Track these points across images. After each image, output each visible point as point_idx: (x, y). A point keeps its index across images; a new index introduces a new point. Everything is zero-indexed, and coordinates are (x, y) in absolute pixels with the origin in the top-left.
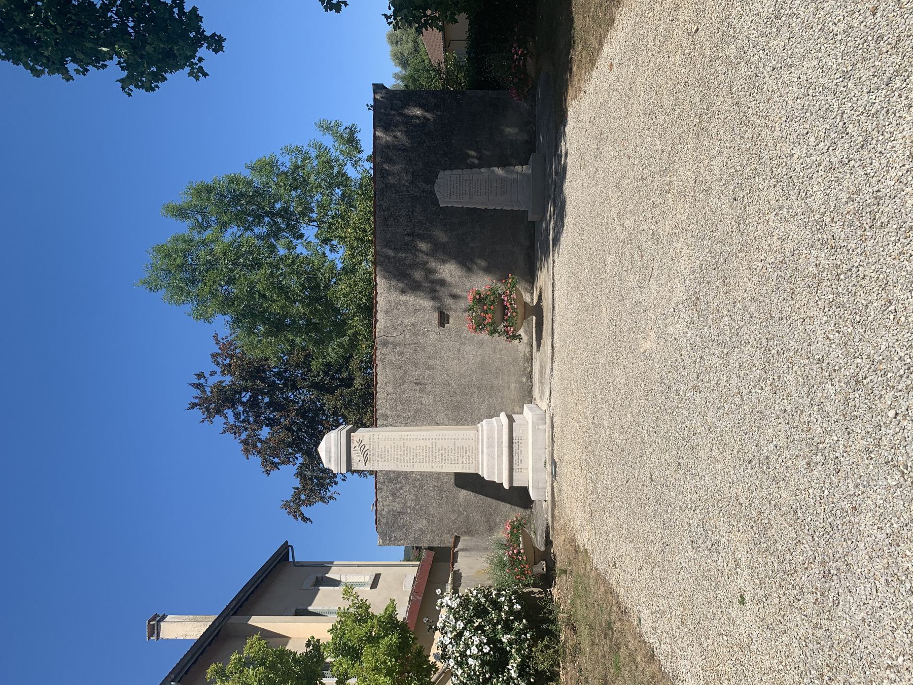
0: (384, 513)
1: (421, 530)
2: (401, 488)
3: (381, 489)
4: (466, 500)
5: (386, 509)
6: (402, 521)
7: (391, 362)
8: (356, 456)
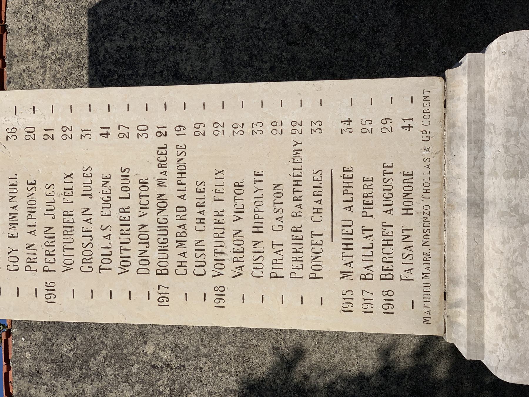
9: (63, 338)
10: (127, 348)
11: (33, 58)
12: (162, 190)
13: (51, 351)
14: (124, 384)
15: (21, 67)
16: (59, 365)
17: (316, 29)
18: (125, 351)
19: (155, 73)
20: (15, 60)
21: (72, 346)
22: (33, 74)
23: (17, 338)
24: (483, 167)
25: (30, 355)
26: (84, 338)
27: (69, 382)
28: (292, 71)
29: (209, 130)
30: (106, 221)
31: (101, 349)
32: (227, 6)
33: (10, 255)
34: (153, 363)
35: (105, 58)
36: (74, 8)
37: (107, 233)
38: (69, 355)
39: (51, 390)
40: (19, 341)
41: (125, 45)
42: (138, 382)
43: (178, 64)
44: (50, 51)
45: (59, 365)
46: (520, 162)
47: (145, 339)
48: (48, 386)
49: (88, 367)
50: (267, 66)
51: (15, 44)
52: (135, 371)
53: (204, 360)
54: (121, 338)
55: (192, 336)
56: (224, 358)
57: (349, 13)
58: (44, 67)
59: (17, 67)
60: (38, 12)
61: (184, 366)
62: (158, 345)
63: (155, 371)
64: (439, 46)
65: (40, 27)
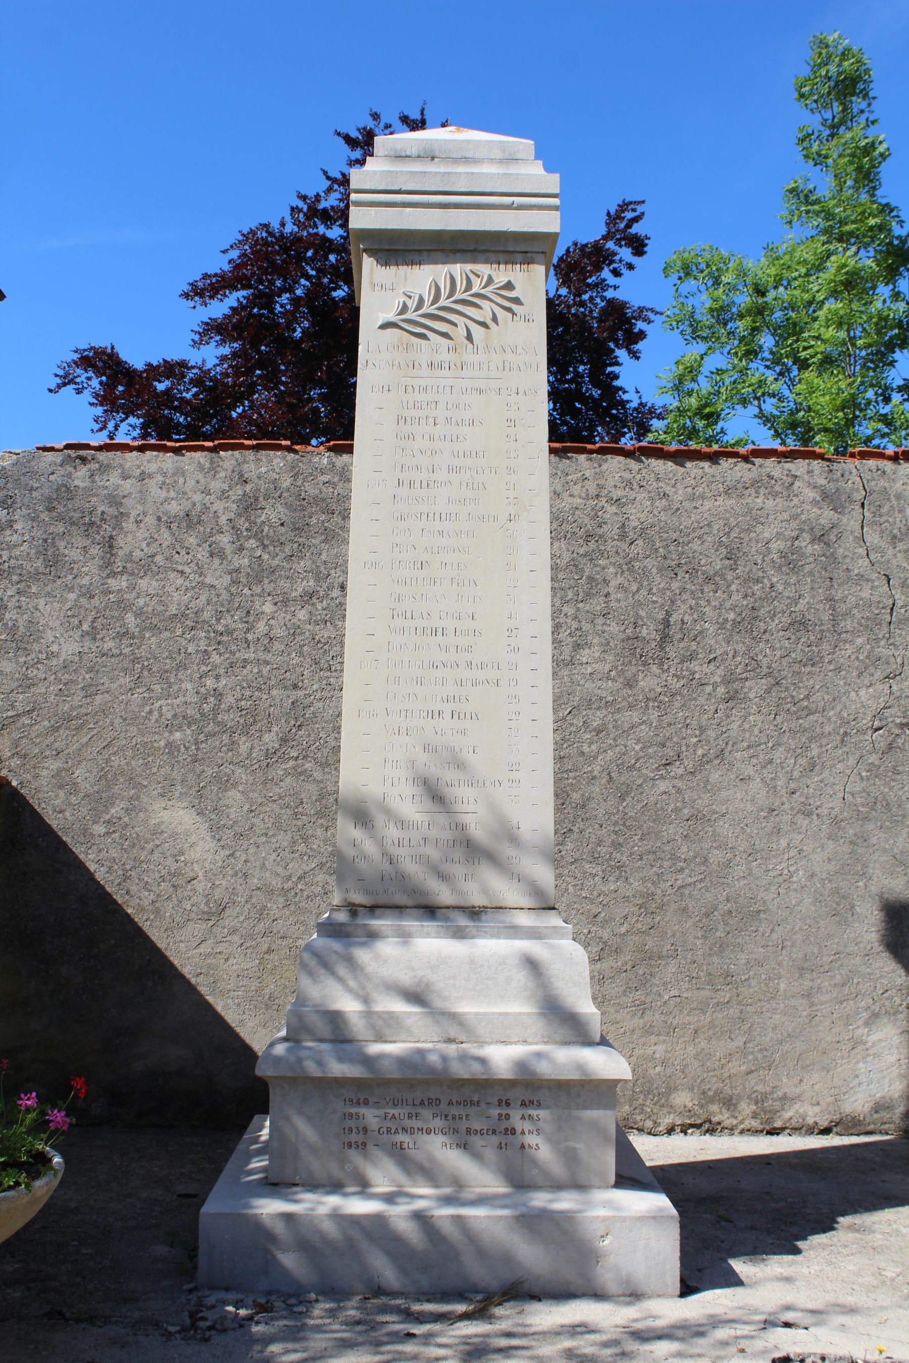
0: (114, 478)
1: (34, 633)
2: (216, 553)
3: (214, 470)
4: (156, 832)
5: (128, 486)
6: (74, 554)
7: (757, 518)
8: (422, 279)
11: (598, 485)
13: (266, 498)
14: (229, 578)
17: (625, 804)
18: (266, 581)
22: (580, 485)
23: (284, 458)
26: (282, 535)
27: (232, 516)
31: (269, 553)
32: (651, 704)
38: (263, 517)
39: (223, 495)
41: (611, 590)
42: (232, 594)
43: (590, 648)
44: (606, 505)
46: (482, 966)
47: (279, 604)
50: (586, 749)
53: (255, 670)
57: (641, 839)
58: (587, 498)
60: (649, 492)
62: (273, 618)
63: (244, 614)
65: (632, 494)
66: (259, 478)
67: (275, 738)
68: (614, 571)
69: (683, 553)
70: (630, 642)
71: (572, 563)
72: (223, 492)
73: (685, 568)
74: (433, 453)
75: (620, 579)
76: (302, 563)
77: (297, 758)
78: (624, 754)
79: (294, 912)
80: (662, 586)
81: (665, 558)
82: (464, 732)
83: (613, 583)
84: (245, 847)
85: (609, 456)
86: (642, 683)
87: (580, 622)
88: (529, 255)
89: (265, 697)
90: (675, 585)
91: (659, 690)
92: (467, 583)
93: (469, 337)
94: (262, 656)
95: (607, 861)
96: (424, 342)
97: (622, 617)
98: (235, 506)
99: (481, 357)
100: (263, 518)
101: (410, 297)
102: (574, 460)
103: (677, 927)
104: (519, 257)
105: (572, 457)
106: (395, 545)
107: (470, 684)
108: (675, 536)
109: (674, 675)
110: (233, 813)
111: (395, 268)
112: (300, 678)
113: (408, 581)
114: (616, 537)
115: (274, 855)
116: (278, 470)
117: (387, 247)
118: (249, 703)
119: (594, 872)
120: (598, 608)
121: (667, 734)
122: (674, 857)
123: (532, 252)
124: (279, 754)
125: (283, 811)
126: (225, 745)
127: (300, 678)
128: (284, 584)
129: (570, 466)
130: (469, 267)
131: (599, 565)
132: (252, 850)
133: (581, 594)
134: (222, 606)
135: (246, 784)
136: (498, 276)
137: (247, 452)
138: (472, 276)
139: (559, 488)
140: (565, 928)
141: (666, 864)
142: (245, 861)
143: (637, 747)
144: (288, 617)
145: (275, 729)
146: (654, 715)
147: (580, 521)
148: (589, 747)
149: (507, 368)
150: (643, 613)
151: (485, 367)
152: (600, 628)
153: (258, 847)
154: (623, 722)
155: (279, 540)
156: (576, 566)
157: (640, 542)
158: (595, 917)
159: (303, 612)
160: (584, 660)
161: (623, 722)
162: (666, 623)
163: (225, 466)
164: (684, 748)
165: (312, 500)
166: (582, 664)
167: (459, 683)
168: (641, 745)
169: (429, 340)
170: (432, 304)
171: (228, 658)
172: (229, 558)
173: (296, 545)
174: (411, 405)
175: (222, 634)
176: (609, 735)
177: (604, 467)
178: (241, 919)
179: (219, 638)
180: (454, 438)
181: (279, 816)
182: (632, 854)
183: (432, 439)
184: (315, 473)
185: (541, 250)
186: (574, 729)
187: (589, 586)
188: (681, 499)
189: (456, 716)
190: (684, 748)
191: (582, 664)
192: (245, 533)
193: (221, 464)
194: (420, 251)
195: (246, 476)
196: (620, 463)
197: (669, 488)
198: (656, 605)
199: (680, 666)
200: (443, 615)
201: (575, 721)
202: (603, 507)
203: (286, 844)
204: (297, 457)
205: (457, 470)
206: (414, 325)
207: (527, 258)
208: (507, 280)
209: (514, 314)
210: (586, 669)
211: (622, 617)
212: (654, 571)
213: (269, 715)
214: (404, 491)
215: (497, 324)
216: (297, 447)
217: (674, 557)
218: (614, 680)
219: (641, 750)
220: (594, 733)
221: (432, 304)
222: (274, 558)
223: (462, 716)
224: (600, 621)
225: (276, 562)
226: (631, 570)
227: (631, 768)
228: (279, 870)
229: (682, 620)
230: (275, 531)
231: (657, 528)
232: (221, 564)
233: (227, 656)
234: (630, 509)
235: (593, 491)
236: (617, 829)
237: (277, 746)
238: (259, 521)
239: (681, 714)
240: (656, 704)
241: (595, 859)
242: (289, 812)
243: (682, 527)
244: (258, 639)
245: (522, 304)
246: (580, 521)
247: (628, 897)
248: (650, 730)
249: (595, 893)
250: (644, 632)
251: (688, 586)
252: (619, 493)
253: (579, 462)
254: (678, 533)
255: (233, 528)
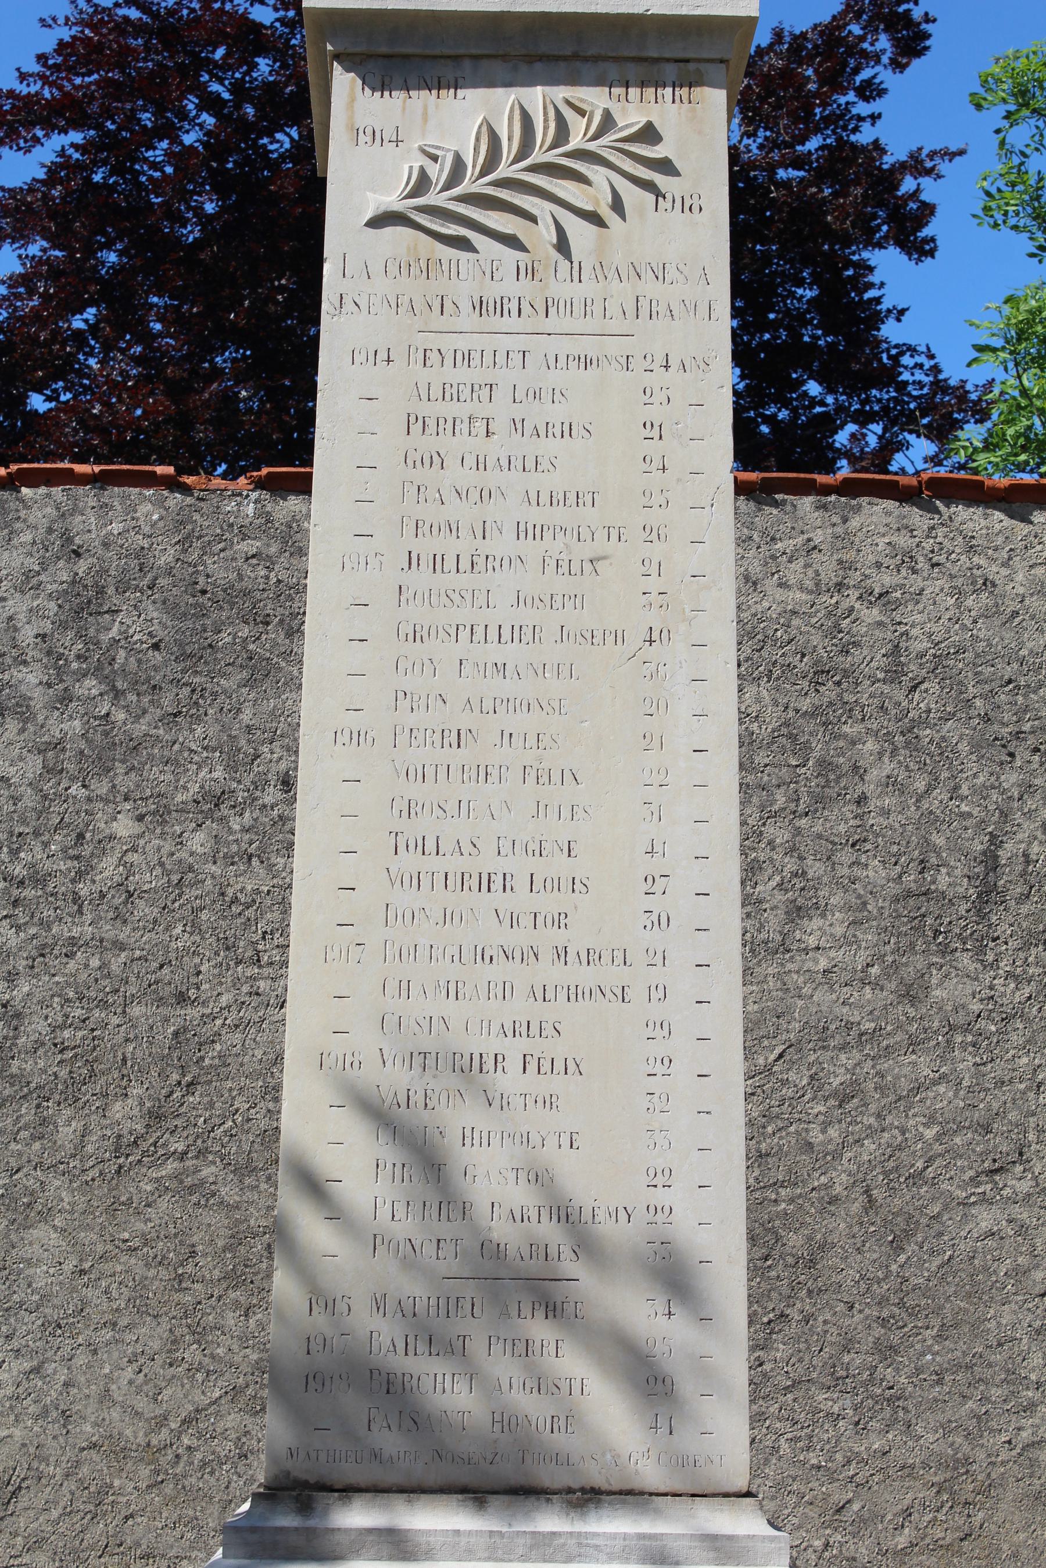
8: (460, 119)
9: (155, 614)
10: (127, 773)
11: (840, 562)
12: (547, 955)
13: (122, 587)
14: (40, 761)
15: (819, 531)
16: (89, 602)
17: (902, 1258)
18: (120, 768)
19: (801, 858)
20: (835, 519)
21: (135, 638)
22: (801, 562)
23: (161, 503)
24: (579, 1562)
25: (116, 532)
26: (156, 668)
27: (47, 626)
28: (800, 1196)
29: (657, 1049)
30: (488, 848)
32: (959, 1039)
33: (427, 662)
34: (88, 835)
35: (837, 737)
36: (961, 665)
37: (467, 847)
38: (115, 629)
39: (28, 582)
40: (150, 506)
41: (870, 789)
42: (45, 797)
43: (823, 915)
44: (857, 606)
45: (89, 602)
47: (148, 818)
48: (38, 573)
49: (84, 676)
50: (816, 1136)
51: (874, 519)
52: (72, 791)
53: (95, 962)
54: (151, 757)
55: (153, 935)
56: (97, 1013)
57: (939, 1337)
58: (818, 590)
59: (819, 523)
60: (952, 577)
61: (80, 912)
62: (134, 849)
64: (854, 1559)
65: (916, 582)
66: (106, 545)
67: (136, 1111)
68: (877, 747)
69: (1026, 709)
70: (911, 902)
71: (784, 731)
72: (28, 575)
73: (1031, 741)
74: (484, 495)
75: (888, 767)
76: (199, 730)
77: (183, 1156)
78: (900, 1148)
79: (173, 1499)
80: (981, 779)
81: (987, 719)
82: (549, 1102)
83: (874, 774)
84: (66, 1351)
85: (864, 500)
86: (937, 993)
87: (801, 858)
88: (692, 66)
89: (115, 1020)
90: (1010, 779)
91: (976, 1007)
92: (556, 777)
93: (563, 246)
94: (109, 932)
95: (865, 1384)
96: (464, 256)
97: (895, 848)
98: (52, 606)
99: (588, 288)
100: (114, 633)
101: (435, 158)
102: (788, 508)
103: (1022, 1536)
104: (670, 71)
105: (784, 502)
106: (401, 695)
107: (562, 996)
108: (1008, 672)
109: (1009, 975)
110: (41, 1278)
111: (403, 94)
112: (193, 980)
113: (430, 772)
114: (880, 675)
115: (129, 1372)
116: (147, 529)
117: (384, 50)
118: (80, 1034)
119: (836, 1409)
120: (842, 828)
121: (995, 1105)
122: (1013, 1378)
123: (699, 60)
124: (144, 1146)
125: (152, 1273)
126: (26, 1127)
127: (193, 980)
128: (160, 776)
129: (780, 522)
130: (561, 93)
131: (845, 736)
132: (82, 1359)
133: (805, 799)
134: (24, 821)
135: (72, 1212)
136: (624, 111)
137: (80, 490)
138: (568, 114)
139: (756, 569)
140: (772, 1539)
141: (995, 1393)
142: (66, 1384)
143: (929, 1133)
144: (168, 846)
145: (136, 1091)
146: (966, 1063)
147: (802, 639)
148: (824, 1131)
149: (644, 311)
150: (939, 840)
151: (598, 309)
152: (845, 871)
153: (95, 1352)
154: (897, 1077)
155: (148, 680)
156: (793, 737)
157: (932, 686)
158: (839, 1510)
159: (200, 836)
160: (812, 941)
161: (897, 1077)
162: (991, 861)
163: (31, 520)
164: (1031, 1136)
165: (221, 595)
166: (807, 951)
167: (539, 995)
168: (936, 1129)
169: (474, 250)
170: (483, 174)
171: (34, 937)
172: (40, 718)
173: (186, 691)
174: (436, 392)
175: (21, 883)
176: (866, 1105)
177: (854, 523)
178: (55, 1514)
179: (15, 892)
180: (530, 464)
181: (142, 1284)
182: (919, 1371)
183: (481, 464)
184: (227, 535)
185: (719, 56)
186: (790, 1093)
187: (822, 781)
188: (1021, 590)
189: (532, 1067)
190: (1031, 1136)
191: (807, 951)
192: (75, 665)
193: (23, 514)
194: (456, 58)
195: (77, 541)
196: (888, 514)
197: (994, 569)
198: (968, 823)
199: (1022, 955)
200: (506, 847)
201: (792, 1076)
202: (851, 609)
203: (156, 1345)
204: (189, 500)
205: (538, 532)
206: (444, 216)
207: (687, 75)
208: (644, 120)
209: (659, 194)
210: (816, 961)
211: (895, 848)
212: (964, 747)
213: (124, 1060)
214: (421, 579)
215: (623, 217)
216: (189, 480)
217: (1006, 717)
218: (877, 986)
219: (938, 1138)
220: (832, 1102)
221: (483, 174)
222: (137, 718)
223: (546, 1066)
224: (845, 856)
225: (142, 727)
226: (913, 745)
227: (916, 1178)
228: (141, 1403)
229: (1026, 855)
230: (139, 661)
231: (969, 655)
232: (22, 731)
233: (33, 931)
234: (913, 615)
235: (829, 573)
236: (885, 1314)
237: (139, 1128)
238: (105, 638)
239: (1025, 1060)
240: (970, 1038)
241: (837, 1382)
242: (164, 1274)
243: (1024, 652)
244: (102, 895)
245: (676, 173)
246: (802, 639)
247: (912, 1467)
248: (956, 1095)
249: (839, 1457)
250: (943, 880)
251: (1037, 782)
252: (887, 579)
253: (800, 513)
254: (1015, 666)
255: (49, 653)
